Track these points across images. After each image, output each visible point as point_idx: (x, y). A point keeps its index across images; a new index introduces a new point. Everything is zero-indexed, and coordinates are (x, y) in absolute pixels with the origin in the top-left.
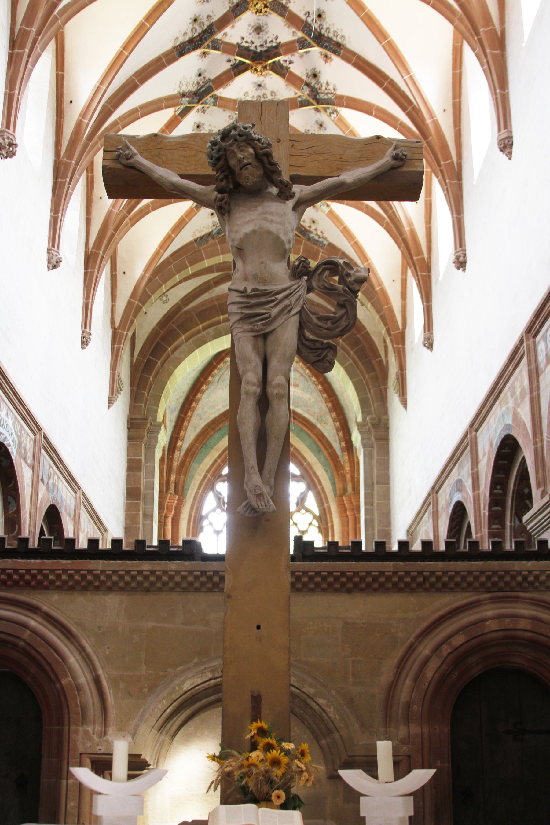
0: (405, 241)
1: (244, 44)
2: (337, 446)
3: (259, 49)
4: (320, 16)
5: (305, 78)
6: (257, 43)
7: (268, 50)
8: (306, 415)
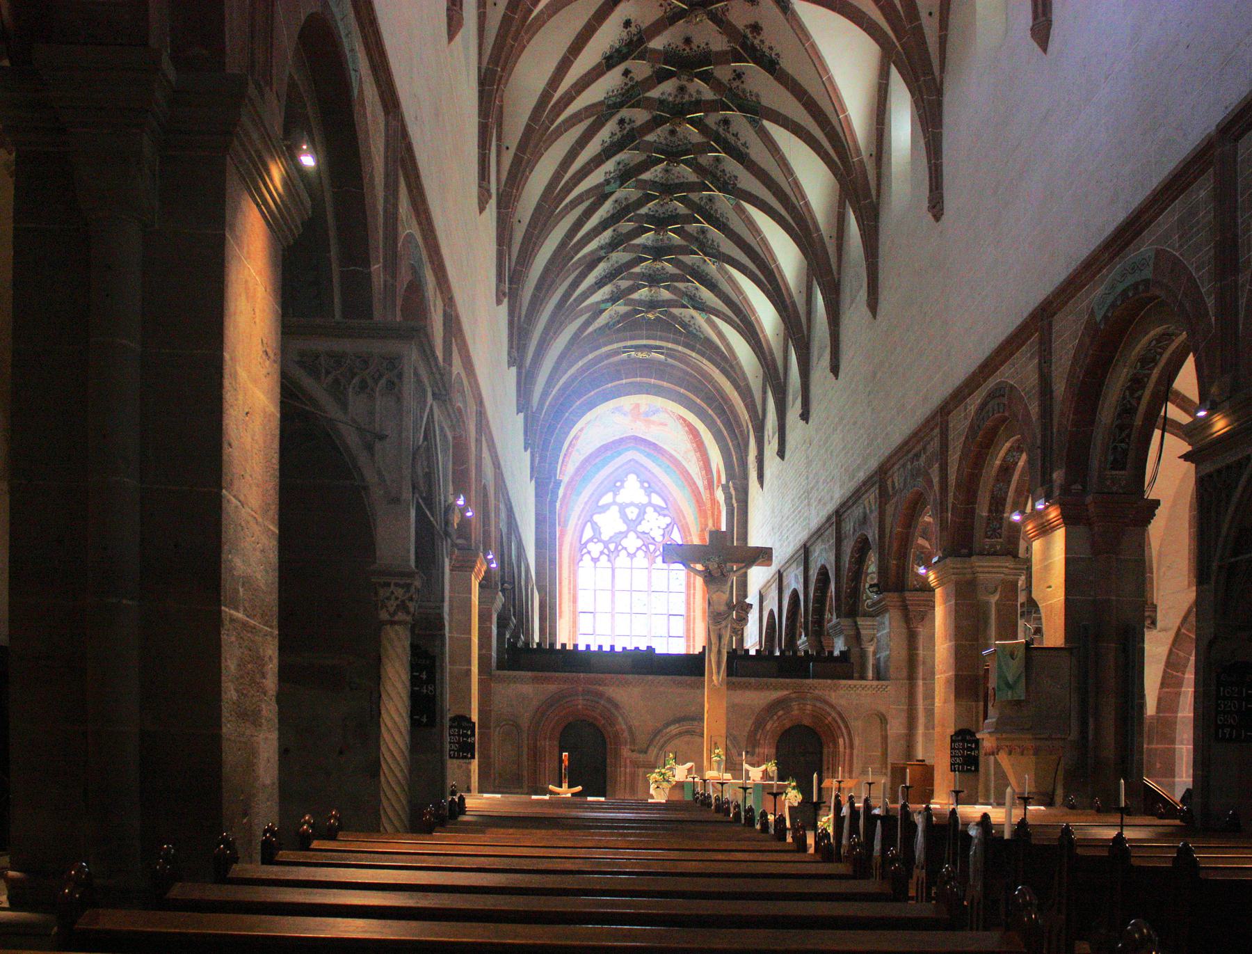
0: (765, 359)
1: (651, 213)
2: (700, 484)
3: (662, 215)
4: (710, 200)
5: (695, 234)
6: (660, 211)
7: (671, 217)
8: (674, 453)
